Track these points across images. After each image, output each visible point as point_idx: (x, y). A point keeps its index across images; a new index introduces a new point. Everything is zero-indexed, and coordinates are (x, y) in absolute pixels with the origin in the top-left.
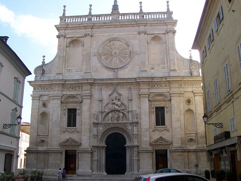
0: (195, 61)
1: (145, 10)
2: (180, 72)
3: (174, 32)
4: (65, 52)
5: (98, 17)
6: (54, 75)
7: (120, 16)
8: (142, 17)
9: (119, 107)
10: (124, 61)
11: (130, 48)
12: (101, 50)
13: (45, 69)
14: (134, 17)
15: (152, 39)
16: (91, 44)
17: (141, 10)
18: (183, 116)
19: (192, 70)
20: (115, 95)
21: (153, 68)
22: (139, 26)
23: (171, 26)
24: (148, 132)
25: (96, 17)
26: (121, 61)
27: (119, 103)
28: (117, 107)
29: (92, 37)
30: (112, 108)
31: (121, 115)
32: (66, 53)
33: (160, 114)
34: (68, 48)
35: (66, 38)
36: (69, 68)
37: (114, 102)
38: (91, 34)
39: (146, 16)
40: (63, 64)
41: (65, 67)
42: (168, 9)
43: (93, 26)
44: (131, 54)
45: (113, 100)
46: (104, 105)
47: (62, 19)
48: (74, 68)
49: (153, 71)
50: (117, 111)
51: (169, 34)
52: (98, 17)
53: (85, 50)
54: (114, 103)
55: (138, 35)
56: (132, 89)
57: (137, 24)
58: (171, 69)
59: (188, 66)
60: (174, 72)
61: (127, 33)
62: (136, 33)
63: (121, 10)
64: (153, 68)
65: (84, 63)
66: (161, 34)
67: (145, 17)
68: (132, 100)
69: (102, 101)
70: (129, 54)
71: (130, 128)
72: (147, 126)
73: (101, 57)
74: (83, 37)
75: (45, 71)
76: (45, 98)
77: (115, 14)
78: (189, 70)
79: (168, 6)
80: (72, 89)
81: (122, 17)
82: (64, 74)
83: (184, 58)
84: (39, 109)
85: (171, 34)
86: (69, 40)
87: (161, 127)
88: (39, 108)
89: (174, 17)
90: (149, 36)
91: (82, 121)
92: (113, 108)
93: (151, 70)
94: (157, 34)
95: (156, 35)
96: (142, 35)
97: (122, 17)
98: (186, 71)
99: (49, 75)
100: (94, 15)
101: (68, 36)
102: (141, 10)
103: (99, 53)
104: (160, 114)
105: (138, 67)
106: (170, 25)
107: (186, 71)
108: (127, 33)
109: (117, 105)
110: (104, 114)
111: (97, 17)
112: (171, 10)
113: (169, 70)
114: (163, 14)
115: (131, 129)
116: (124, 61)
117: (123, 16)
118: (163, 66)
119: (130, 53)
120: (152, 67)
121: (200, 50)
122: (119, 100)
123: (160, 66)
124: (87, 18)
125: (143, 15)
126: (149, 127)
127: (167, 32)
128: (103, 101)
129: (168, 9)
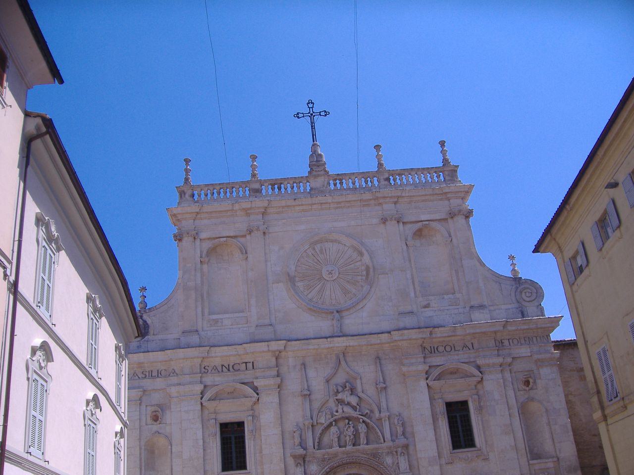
0: (526, 281)
1: (389, 166)
2: (495, 310)
3: (468, 214)
4: (199, 275)
5: (275, 184)
6: (176, 336)
7: (331, 182)
8: (386, 182)
9: (354, 408)
10: (354, 291)
11: (366, 258)
12: (293, 268)
13: (149, 321)
14: (366, 182)
15: (415, 234)
16: (265, 254)
17: (380, 165)
18: (518, 417)
19: (524, 303)
20: (340, 378)
21: (429, 304)
22: (380, 204)
23: (459, 201)
24: (437, 468)
25: (270, 186)
26: (346, 292)
27: (353, 400)
28: (348, 411)
29: (267, 236)
30: (337, 412)
31: (362, 428)
32: (202, 278)
33: (458, 418)
34: (205, 267)
35: (198, 242)
36: (214, 317)
37: (340, 396)
38: (262, 228)
39: (395, 180)
40: (196, 307)
41: (203, 315)
42: (445, 161)
43: (266, 208)
44: (370, 275)
45: (338, 392)
46: (316, 405)
47: (185, 194)
48: (227, 316)
49: (428, 313)
50: (349, 419)
51: (455, 219)
52: (276, 186)
53: (252, 270)
54: (340, 402)
55: (382, 226)
56: (383, 362)
57: (377, 198)
58: (472, 303)
59: (513, 294)
60: (481, 311)
61: (353, 223)
62: (375, 221)
63: (333, 168)
64: (429, 304)
65: (253, 301)
66: (436, 220)
67: (392, 181)
68: (385, 388)
69: (309, 395)
70: (364, 273)
71: (389, 460)
72: (433, 452)
73: (295, 285)
74: (244, 236)
75: (148, 327)
76: (156, 398)
77: (319, 176)
78: (516, 305)
79: (443, 152)
80: (229, 370)
81: (335, 185)
82: (203, 333)
83: (499, 276)
84: (140, 429)
85: (460, 220)
86: (207, 245)
87: (465, 453)
88: (140, 427)
89: (464, 178)
90: (409, 226)
91: (264, 452)
92: (340, 411)
93: (423, 309)
94: (427, 223)
95: (424, 223)
96: (392, 226)
97: (335, 185)
98: (510, 306)
99: (160, 337)
100: (265, 181)
101: (203, 235)
102: (380, 165)
103: (289, 275)
104: (458, 418)
105: (390, 304)
106: (457, 198)
107: (510, 306)
108: (353, 223)
109: (349, 404)
110: (319, 430)
111: (273, 185)
112: (453, 163)
113: (468, 309)
114: (435, 172)
115: (393, 463)
116: (354, 291)
117: (338, 182)
118: (450, 298)
119: (367, 269)
120: (425, 303)
121: (559, 251)
122: (353, 391)
123: (443, 298)
124: (247, 189)
125: (386, 176)
126: (437, 454)
127: (452, 215)
128: (313, 397)
129: (445, 161)
